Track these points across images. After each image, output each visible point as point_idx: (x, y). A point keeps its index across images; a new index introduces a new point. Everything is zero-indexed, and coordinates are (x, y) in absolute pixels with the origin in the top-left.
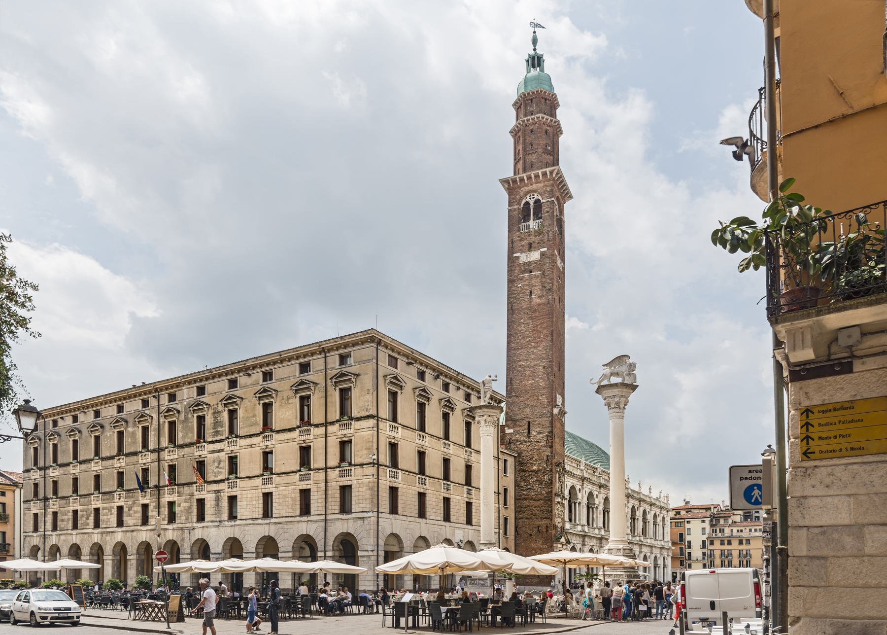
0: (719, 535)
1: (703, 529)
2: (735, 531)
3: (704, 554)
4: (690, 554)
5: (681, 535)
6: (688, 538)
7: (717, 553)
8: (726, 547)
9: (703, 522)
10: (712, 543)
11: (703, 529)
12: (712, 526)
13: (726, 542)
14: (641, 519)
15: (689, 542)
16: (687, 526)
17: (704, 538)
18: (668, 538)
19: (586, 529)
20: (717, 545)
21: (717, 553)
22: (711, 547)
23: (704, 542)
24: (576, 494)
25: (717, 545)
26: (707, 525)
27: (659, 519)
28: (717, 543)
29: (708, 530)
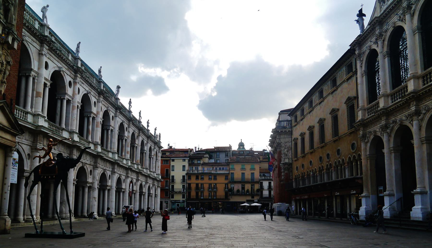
0: (196, 172)
1: (184, 166)
2: (206, 169)
3: (183, 186)
4: (173, 186)
5: (167, 171)
6: (172, 173)
7: (193, 186)
8: (200, 181)
9: (184, 160)
10: (189, 178)
11: (184, 166)
12: (189, 165)
13: (200, 178)
14: (139, 148)
15: (173, 177)
16: (172, 163)
17: (184, 173)
18: (159, 172)
19: (76, 138)
20: (193, 180)
21: (193, 186)
22: (189, 182)
23: (184, 177)
24: (64, 87)
25: (193, 180)
26: (186, 163)
27: (153, 153)
28: (193, 179)
29: (187, 168)
